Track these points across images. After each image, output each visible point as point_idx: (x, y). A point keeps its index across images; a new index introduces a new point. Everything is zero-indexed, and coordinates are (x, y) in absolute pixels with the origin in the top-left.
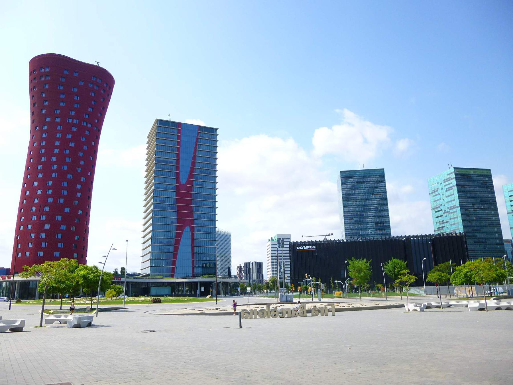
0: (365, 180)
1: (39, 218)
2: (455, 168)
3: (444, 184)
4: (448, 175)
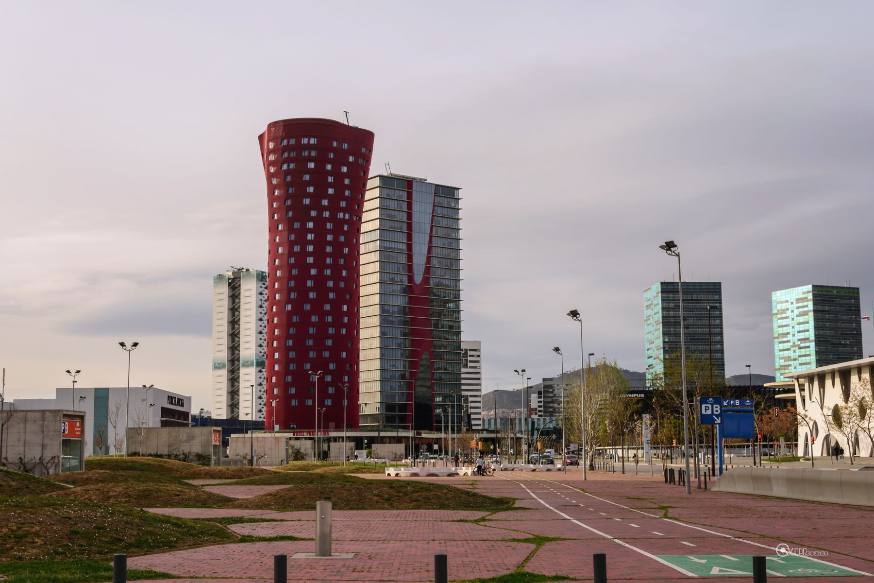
0: (695, 297)
1: (319, 354)
2: (813, 286)
3: (796, 305)
4: (803, 293)
